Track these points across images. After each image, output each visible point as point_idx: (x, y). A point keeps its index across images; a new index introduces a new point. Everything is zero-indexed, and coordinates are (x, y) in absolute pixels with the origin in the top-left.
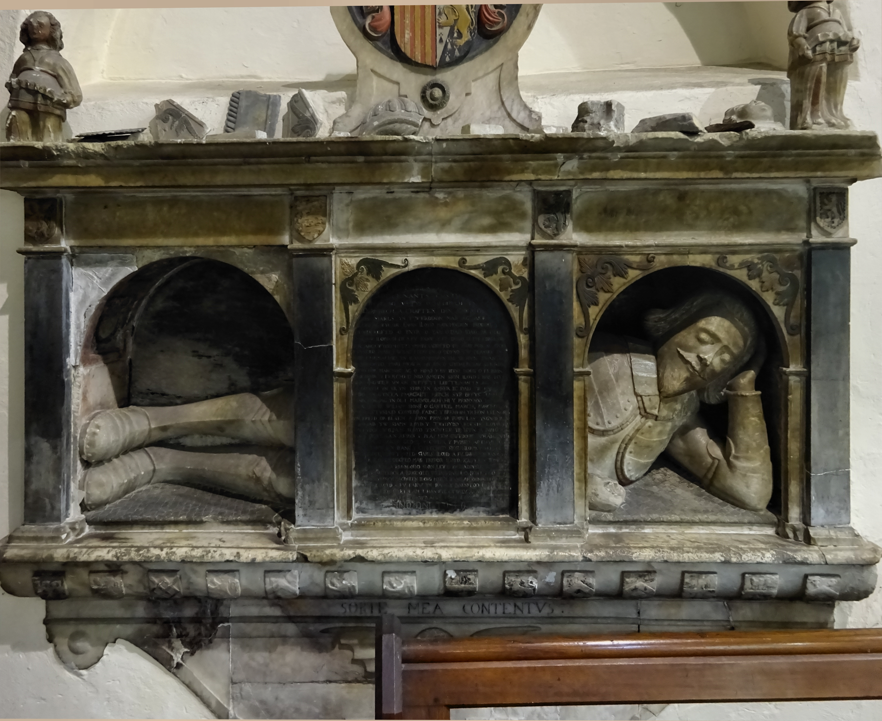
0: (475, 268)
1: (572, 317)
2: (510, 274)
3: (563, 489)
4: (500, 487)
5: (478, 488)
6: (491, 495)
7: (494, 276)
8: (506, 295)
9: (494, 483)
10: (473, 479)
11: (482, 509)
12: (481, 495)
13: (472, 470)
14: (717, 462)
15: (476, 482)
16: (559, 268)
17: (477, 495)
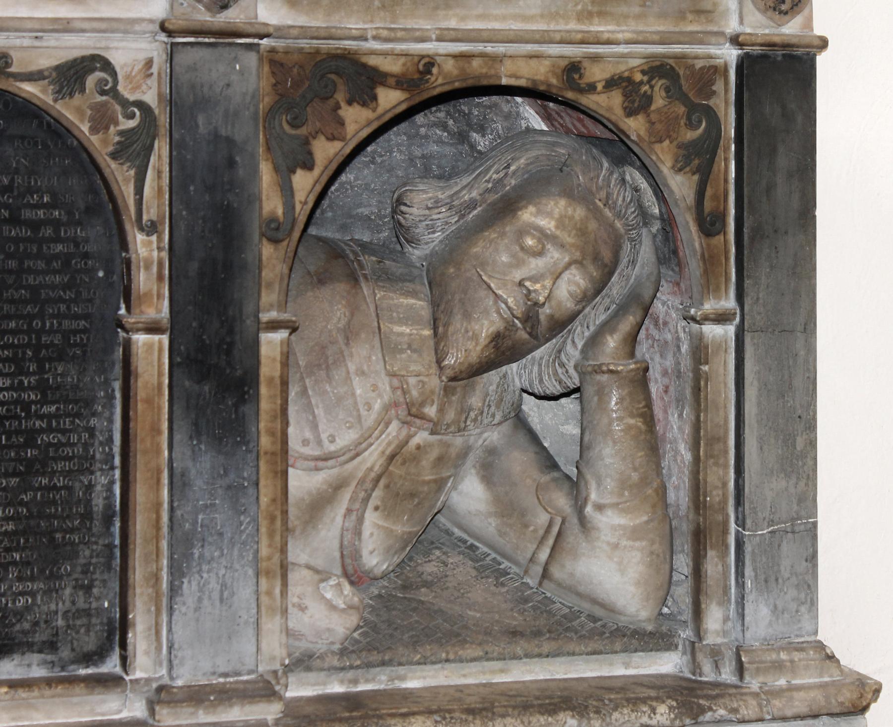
0: (31, 77)
1: (255, 199)
2: (114, 92)
3: (233, 594)
4: (81, 603)
5: (28, 608)
6: (60, 622)
7: (77, 99)
8: (105, 142)
9: (68, 591)
10: (18, 587)
11: (36, 657)
12: (36, 624)
13: (14, 563)
14: (558, 520)
15: (22, 594)
16: (228, 85)
17: (27, 626)
